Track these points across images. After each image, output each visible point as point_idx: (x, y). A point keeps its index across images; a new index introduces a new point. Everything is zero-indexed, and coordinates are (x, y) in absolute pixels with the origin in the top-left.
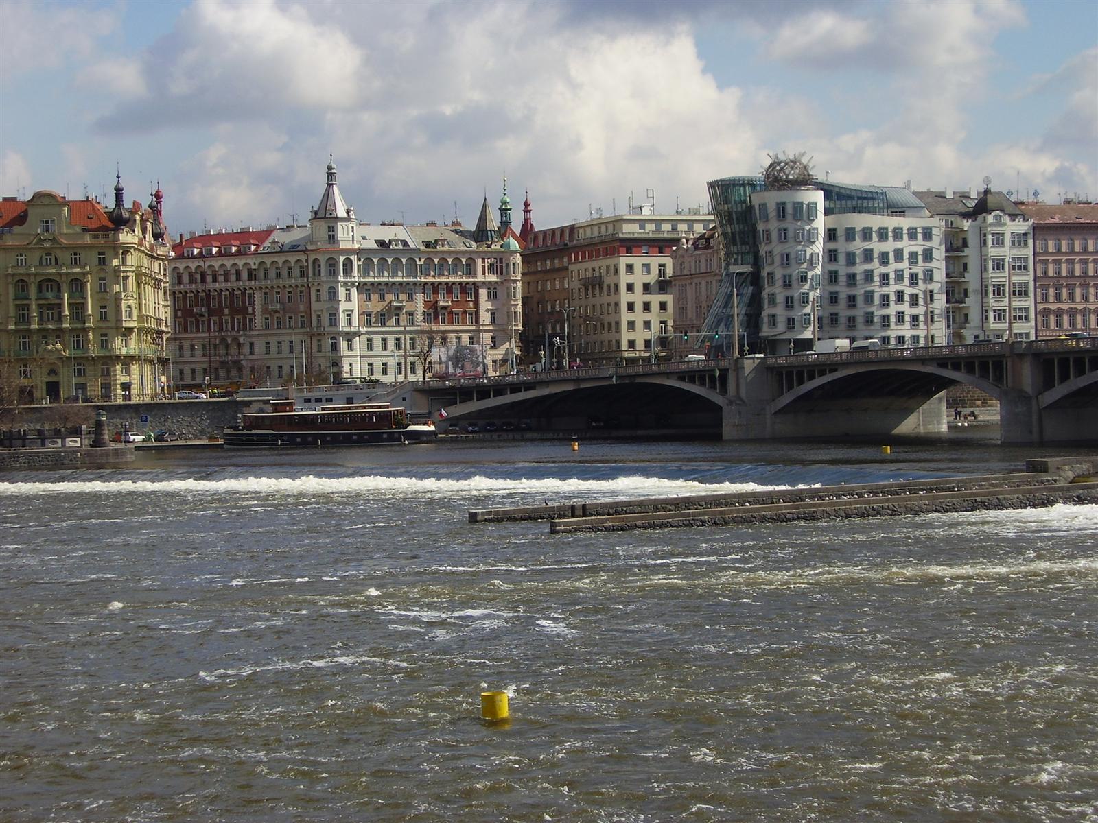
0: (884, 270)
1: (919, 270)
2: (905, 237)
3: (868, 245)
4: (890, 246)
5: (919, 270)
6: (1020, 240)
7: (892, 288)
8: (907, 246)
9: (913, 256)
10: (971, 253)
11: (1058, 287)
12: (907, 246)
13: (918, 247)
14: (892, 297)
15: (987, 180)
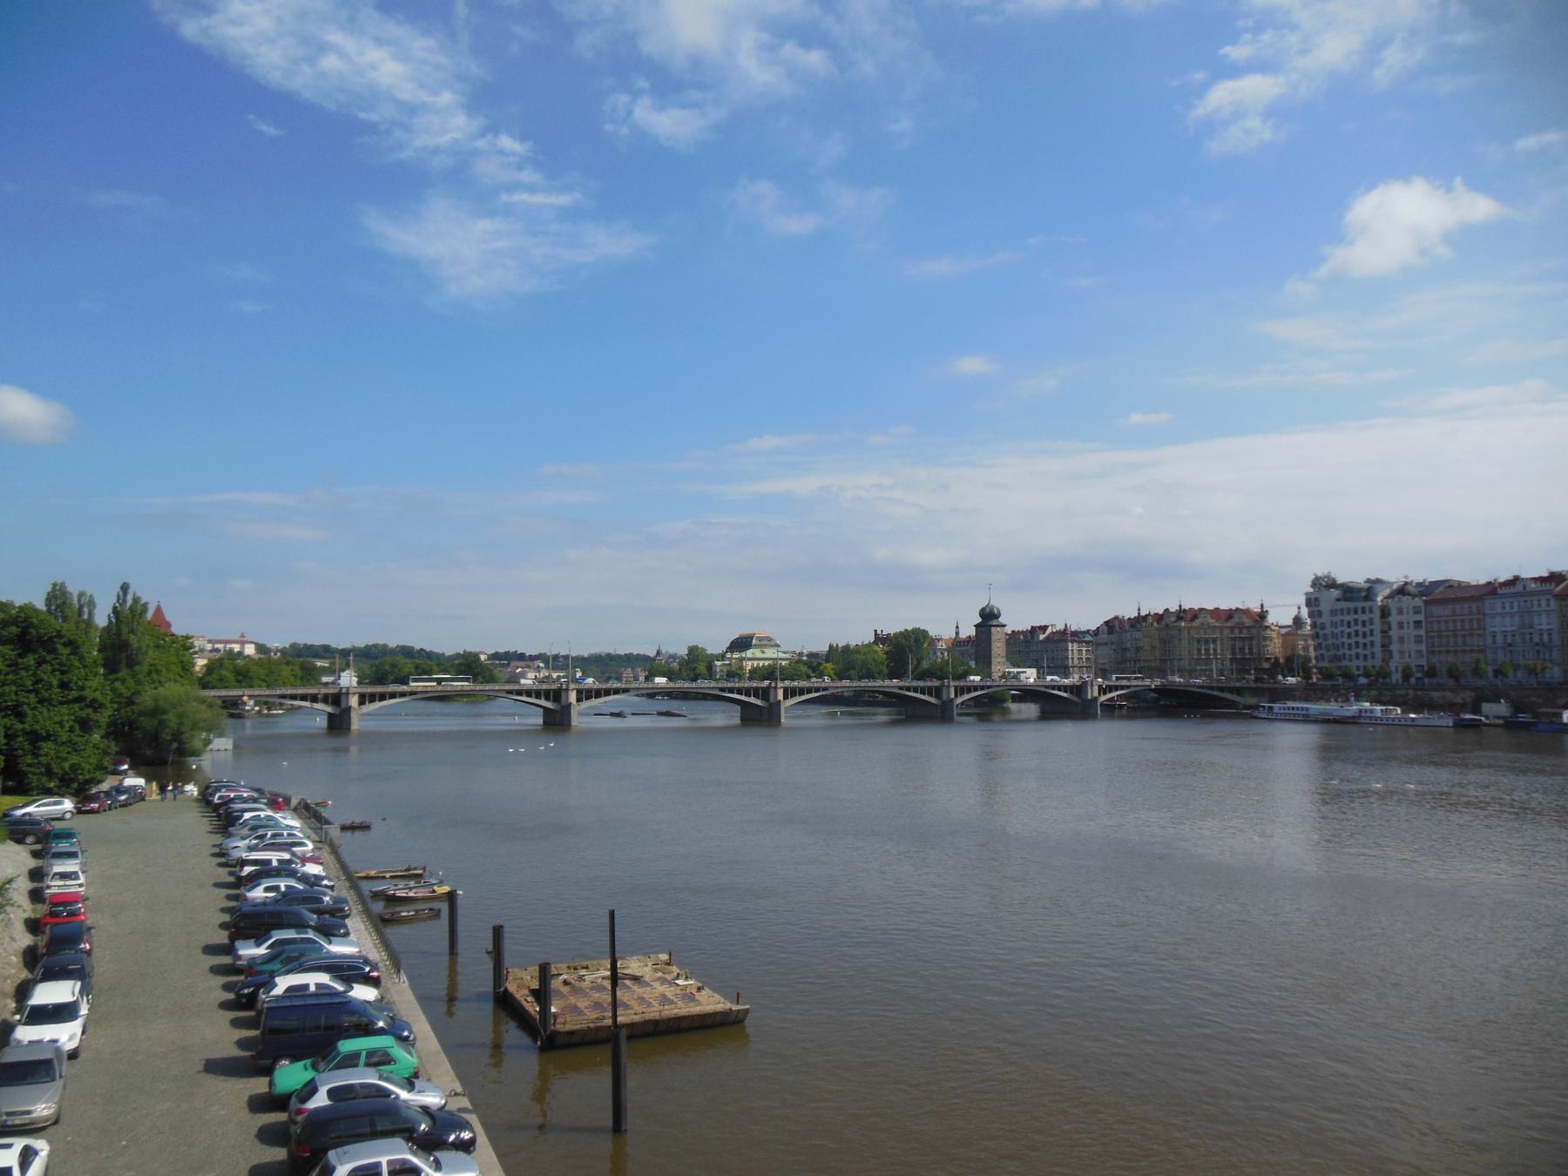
0: (1349, 630)
1: (1367, 630)
2: (1360, 612)
3: (1342, 617)
4: (1351, 617)
5: (1367, 630)
6: (1417, 611)
7: (1353, 641)
8: (1361, 617)
9: (1364, 623)
10: (1394, 618)
11: (1440, 637)
12: (1361, 617)
13: (1366, 617)
14: (1353, 645)
15: (1406, 577)
